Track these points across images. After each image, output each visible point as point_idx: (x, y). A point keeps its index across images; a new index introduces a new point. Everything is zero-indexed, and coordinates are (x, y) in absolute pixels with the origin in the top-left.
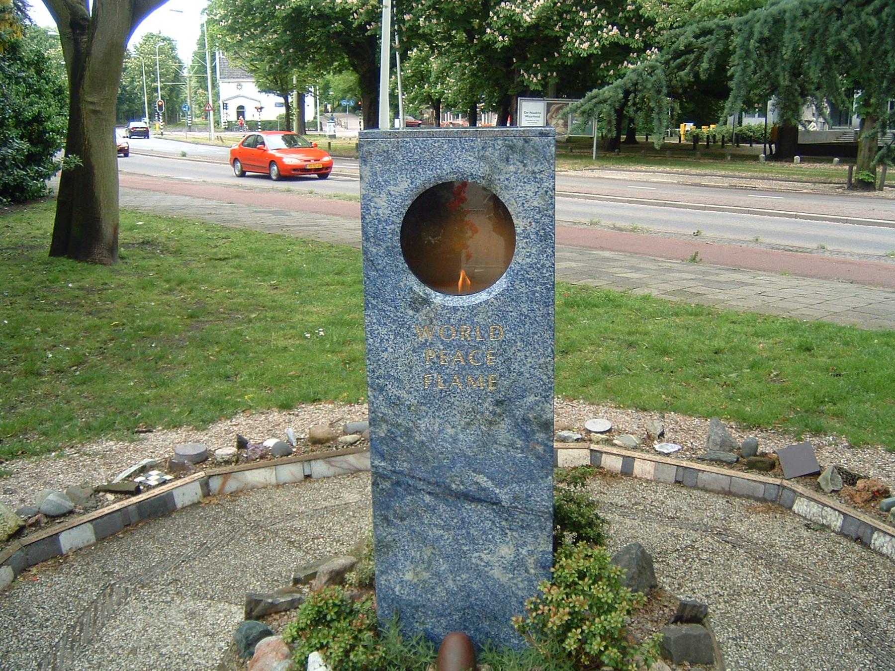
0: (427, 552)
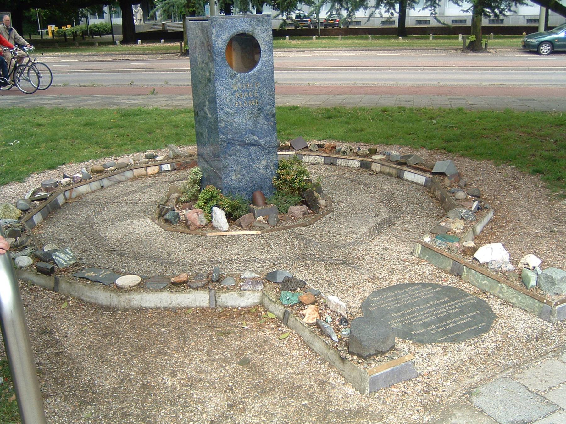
0: (239, 167)
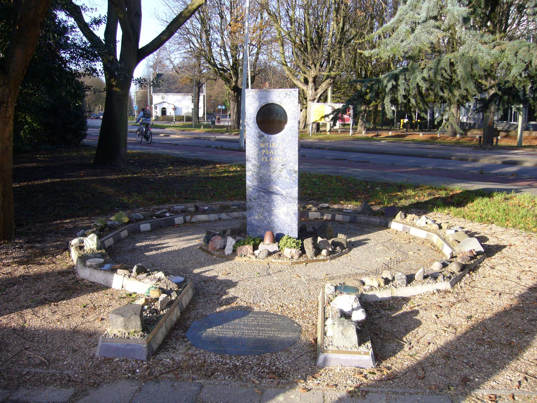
0: (262, 210)
